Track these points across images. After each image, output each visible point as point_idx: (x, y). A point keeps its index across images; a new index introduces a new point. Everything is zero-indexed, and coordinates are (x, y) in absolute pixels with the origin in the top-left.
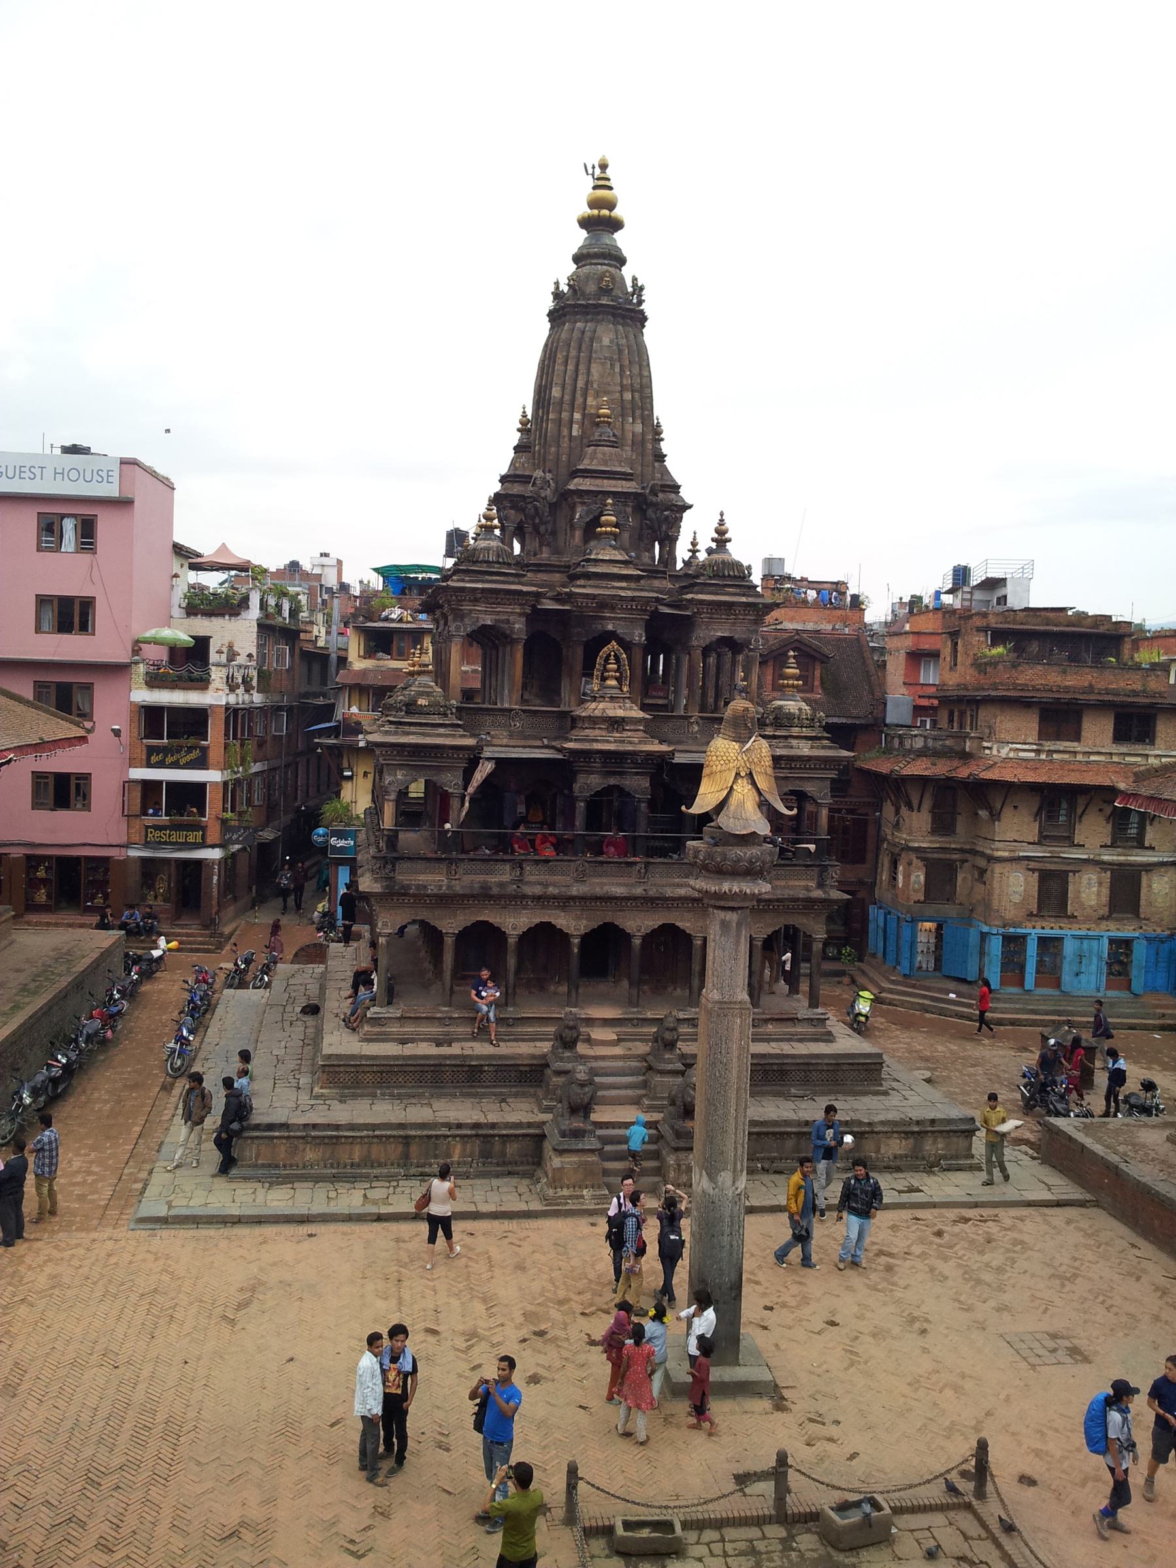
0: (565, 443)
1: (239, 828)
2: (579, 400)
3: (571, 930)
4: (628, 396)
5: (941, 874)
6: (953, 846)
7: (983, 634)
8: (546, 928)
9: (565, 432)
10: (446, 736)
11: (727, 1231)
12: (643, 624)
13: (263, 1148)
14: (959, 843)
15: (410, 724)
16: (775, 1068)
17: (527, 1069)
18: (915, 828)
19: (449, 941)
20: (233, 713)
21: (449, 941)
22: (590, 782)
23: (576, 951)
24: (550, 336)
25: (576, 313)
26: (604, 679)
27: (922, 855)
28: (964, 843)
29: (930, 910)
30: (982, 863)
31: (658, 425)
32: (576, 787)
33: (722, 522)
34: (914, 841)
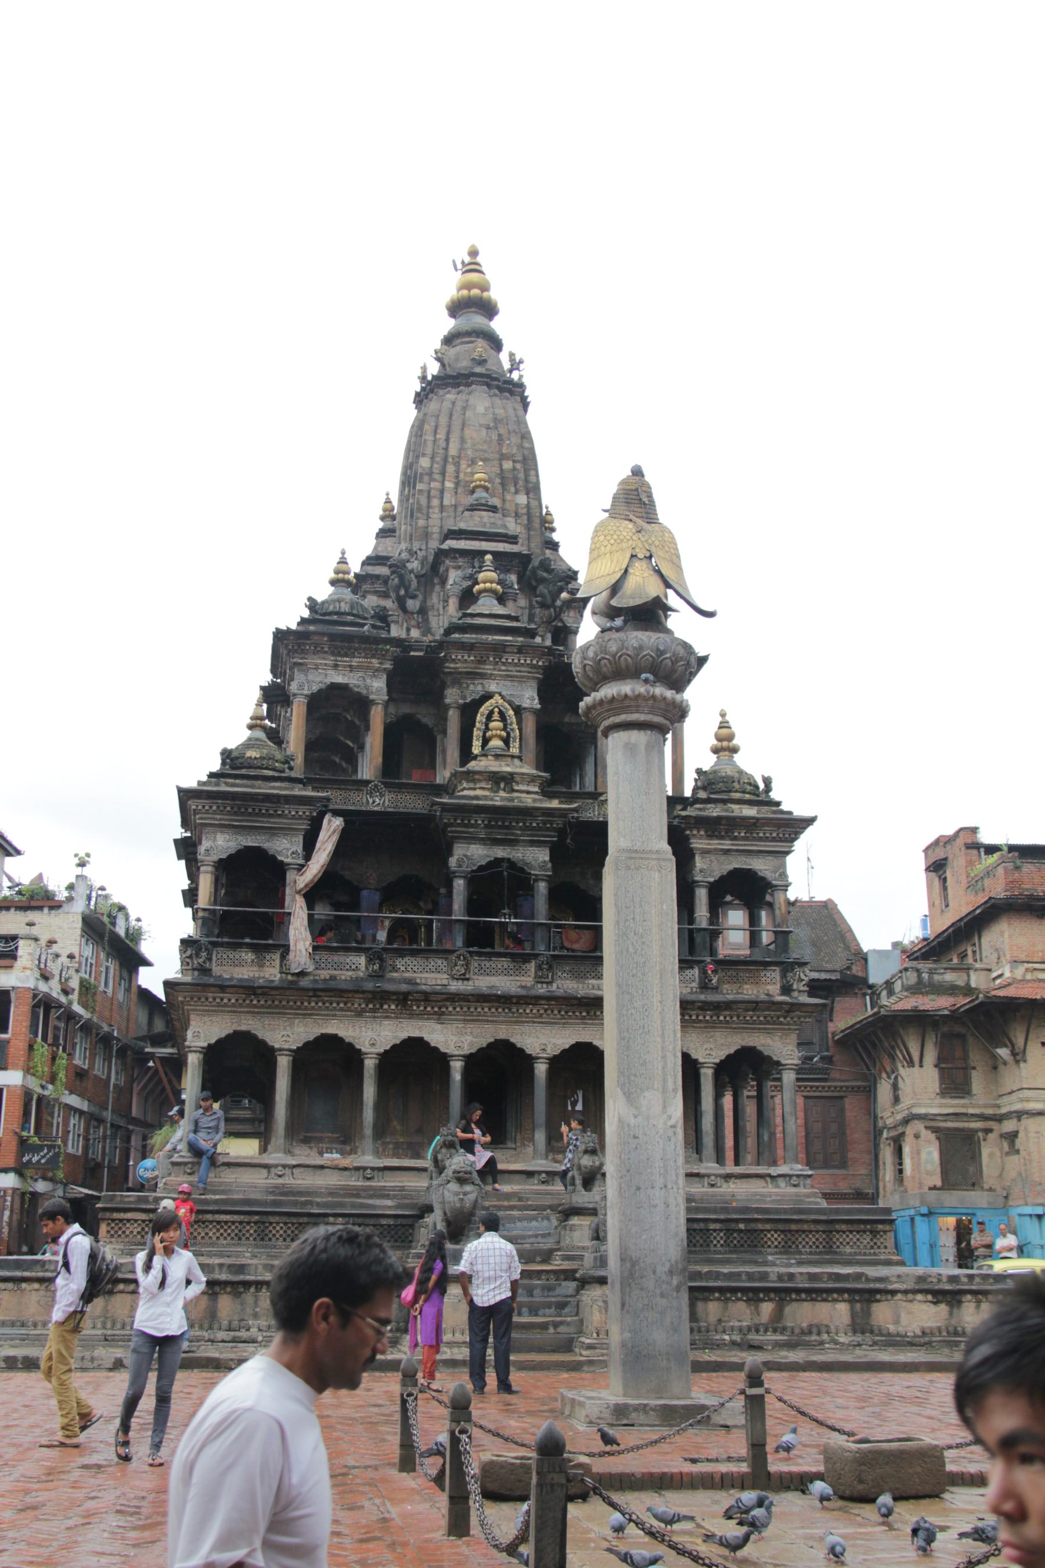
0: (435, 514)
1: (40, 1148)
2: (451, 469)
4: (508, 465)
5: (960, 1150)
6: (971, 1111)
7: (975, 852)
8: (415, 1046)
9: (435, 502)
10: (286, 789)
11: (659, 1182)
12: (534, 685)
14: (979, 1106)
15: (236, 777)
16: (742, 1226)
17: (391, 1222)
18: (916, 1085)
19: (283, 1063)
20: (43, 1005)
21: (283, 1063)
22: (470, 854)
23: (457, 1076)
24: (418, 431)
25: (446, 385)
26: (485, 741)
27: (932, 1124)
28: (986, 1106)
29: (952, 1198)
30: (1009, 1126)
31: (548, 514)
32: (453, 862)
34: (919, 1105)
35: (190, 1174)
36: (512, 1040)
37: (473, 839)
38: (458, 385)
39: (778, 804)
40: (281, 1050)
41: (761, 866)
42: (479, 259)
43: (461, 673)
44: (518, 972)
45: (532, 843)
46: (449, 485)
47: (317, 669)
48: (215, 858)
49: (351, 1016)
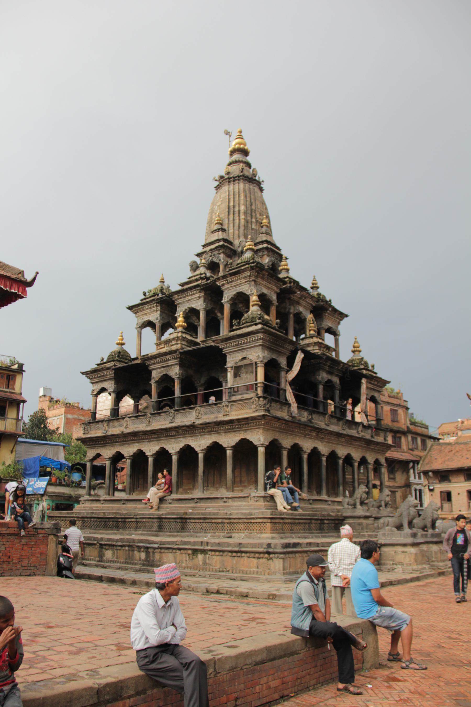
2: (254, 214)
3: (323, 453)
9: (250, 225)
13: (292, 560)
21: (285, 453)
22: (323, 376)
23: (324, 463)
26: (310, 330)
33: (314, 280)
35: (268, 501)
36: (336, 451)
37: (324, 370)
38: (250, 182)
39: (376, 373)
40: (285, 448)
41: (376, 395)
42: (242, 134)
43: (294, 301)
44: (337, 425)
45: (337, 376)
46: (254, 220)
47: (259, 285)
48: (266, 361)
49: (301, 436)
